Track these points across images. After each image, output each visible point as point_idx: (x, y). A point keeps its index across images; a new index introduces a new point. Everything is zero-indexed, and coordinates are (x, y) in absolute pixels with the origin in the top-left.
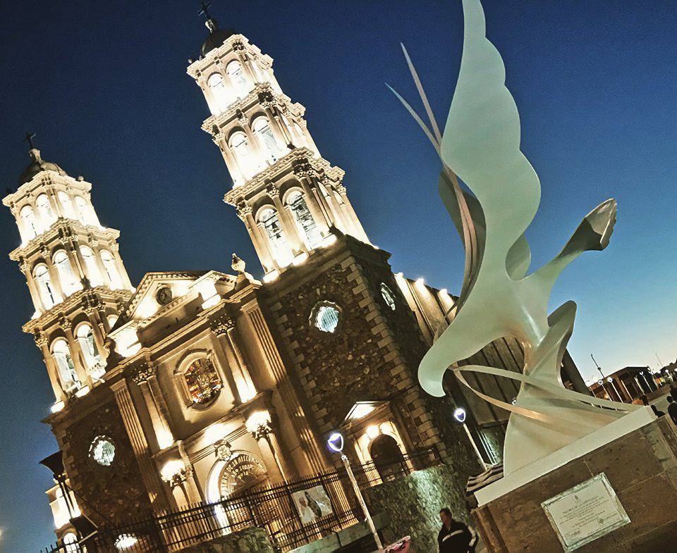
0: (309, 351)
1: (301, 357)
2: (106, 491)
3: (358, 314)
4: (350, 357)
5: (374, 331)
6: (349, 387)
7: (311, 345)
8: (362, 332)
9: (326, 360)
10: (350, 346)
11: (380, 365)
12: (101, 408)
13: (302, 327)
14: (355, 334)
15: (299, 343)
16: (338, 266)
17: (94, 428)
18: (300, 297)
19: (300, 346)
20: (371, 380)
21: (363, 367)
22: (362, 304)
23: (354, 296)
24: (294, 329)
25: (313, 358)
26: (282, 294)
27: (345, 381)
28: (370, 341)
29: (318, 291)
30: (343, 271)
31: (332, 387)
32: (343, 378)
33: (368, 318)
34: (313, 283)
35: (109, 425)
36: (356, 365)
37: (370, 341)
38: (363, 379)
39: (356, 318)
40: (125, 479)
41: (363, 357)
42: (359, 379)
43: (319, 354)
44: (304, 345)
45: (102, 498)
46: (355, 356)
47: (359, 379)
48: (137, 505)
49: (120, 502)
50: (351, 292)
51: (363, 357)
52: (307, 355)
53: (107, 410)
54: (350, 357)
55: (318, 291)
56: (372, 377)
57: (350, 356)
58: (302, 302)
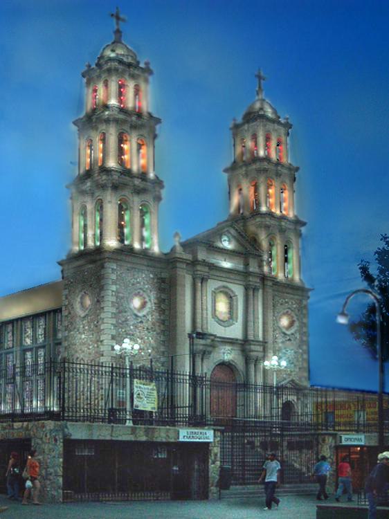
48: (150, 351)
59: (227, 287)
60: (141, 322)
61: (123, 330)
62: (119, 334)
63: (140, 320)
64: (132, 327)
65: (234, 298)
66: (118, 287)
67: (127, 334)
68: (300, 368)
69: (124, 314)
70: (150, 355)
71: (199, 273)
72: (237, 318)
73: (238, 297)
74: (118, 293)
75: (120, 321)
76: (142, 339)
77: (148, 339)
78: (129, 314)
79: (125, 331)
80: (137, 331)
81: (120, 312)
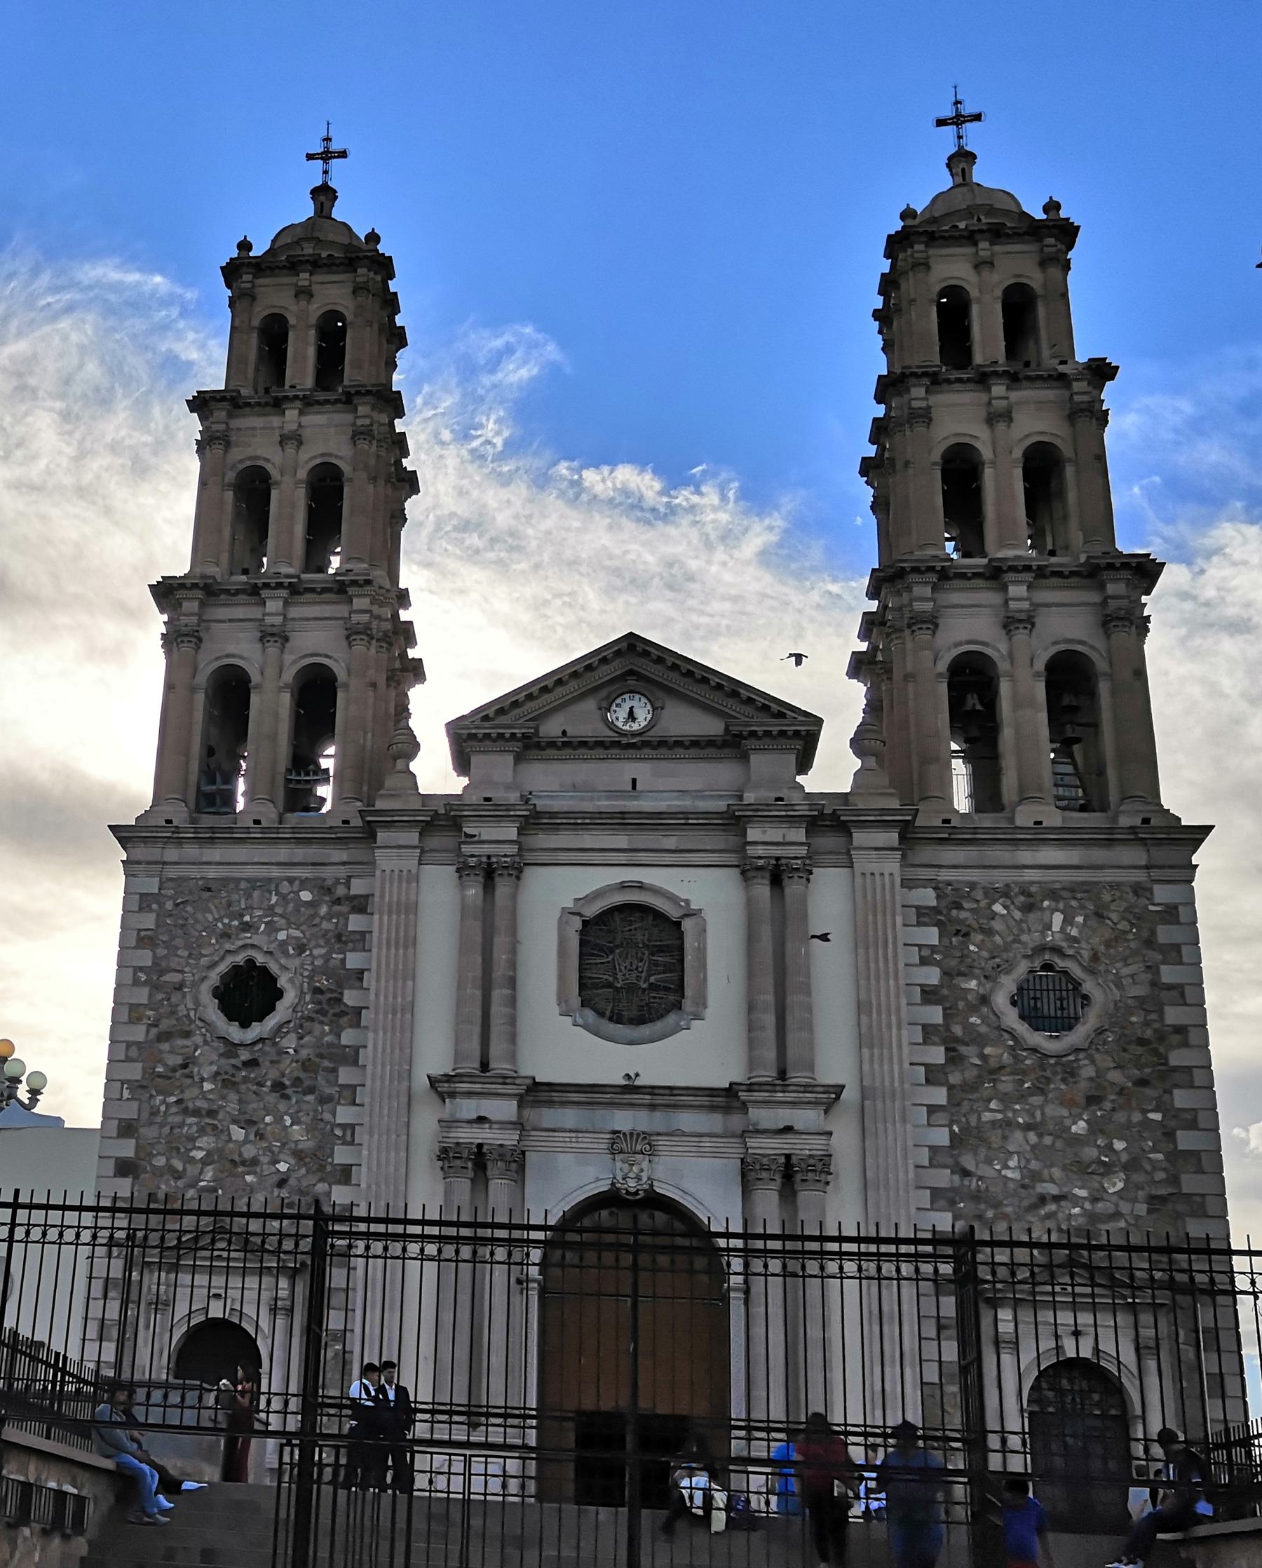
0: (963, 1050)
1: (937, 1055)
2: (207, 1086)
3: (1149, 1033)
4: (1080, 1127)
6: (1043, 1200)
7: (979, 1040)
8: (1142, 1082)
9: (1006, 1099)
10: (1093, 1100)
11: (1163, 1192)
12: (291, 880)
13: (973, 984)
14: (1115, 1076)
15: (945, 1016)
17: (247, 918)
18: (998, 908)
19: (947, 1025)
20: (1117, 1215)
21: (1108, 1170)
23: (1155, 984)
24: (946, 973)
25: (971, 1074)
26: (945, 875)
27: (1036, 1177)
28: (1156, 1116)
29: (1058, 919)
30: (1152, 908)
31: (994, 1174)
32: (1034, 1165)
34: (1053, 895)
35: (297, 933)
36: (1090, 1153)
37: (1156, 1116)
38: (1095, 1200)
39: (1142, 1042)
40: (278, 1086)
41: (1119, 1145)
42: (1082, 1193)
43: (995, 1072)
44: (957, 1030)
45: (187, 1095)
46: (1095, 1128)
47: (1082, 1193)
48: (283, 1167)
49: (238, 1133)
50: (1152, 969)
51: (1119, 1145)
52: (954, 1058)
53: (306, 896)
54: (1080, 1127)
56: (1125, 1208)
57: (1082, 1124)
58: (997, 925)
59: (640, 886)
60: (252, 1063)
61: (173, 1099)
62: (154, 1112)
63: (245, 1055)
64: (207, 1086)
65: (687, 925)
66: (161, 952)
67: (186, 1112)
68: (1152, 1200)
69: (180, 1042)
70: (282, 1183)
71: (760, 851)
72: (702, 1002)
73: (708, 916)
74: (162, 972)
75: (160, 1069)
76: (248, 1123)
77: (278, 1120)
78: (198, 1039)
79: (179, 1102)
80: (233, 1097)
81: (165, 1036)
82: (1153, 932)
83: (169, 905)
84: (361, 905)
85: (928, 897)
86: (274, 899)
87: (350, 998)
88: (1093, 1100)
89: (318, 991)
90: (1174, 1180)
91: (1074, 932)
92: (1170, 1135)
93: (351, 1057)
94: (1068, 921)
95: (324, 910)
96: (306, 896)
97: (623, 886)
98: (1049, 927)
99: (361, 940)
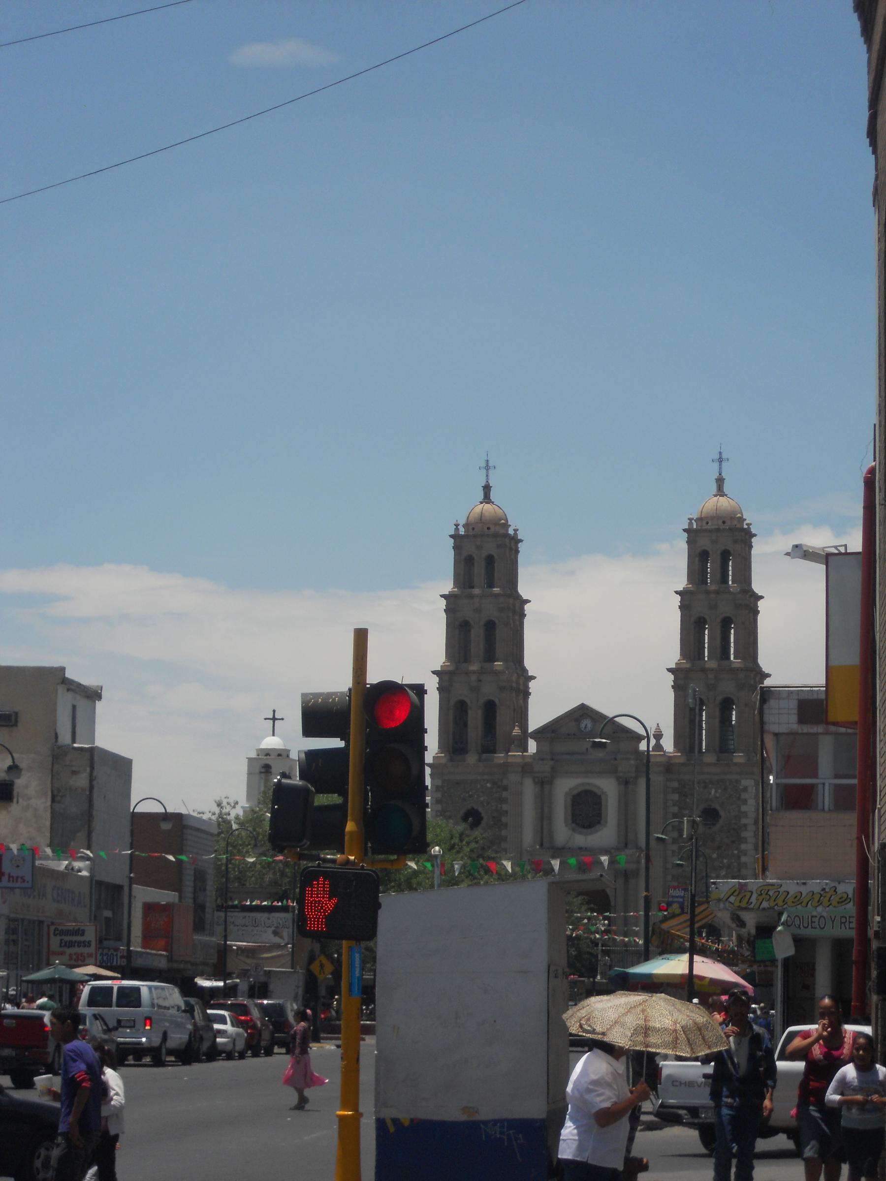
5: (743, 847)
8: (733, 842)
16: (738, 781)
17: (470, 793)
22: (744, 821)
29: (713, 791)
33: (743, 834)
37: (736, 852)
41: (725, 861)
50: (739, 807)
51: (725, 861)
54: (715, 856)
55: (713, 791)
59: (589, 784)
72: (606, 822)
82: (740, 795)
83: (445, 789)
84: (505, 788)
85: (675, 784)
86: (479, 786)
87: (504, 820)
88: (719, 848)
89: (494, 817)
90: (739, 871)
91: (718, 795)
92: (739, 857)
93: (505, 839)
94: (716, 792)
95: (494, 790)
96: (489, 785)
97: (582, 784)
98: (710, 793)
99: (505, 801)
